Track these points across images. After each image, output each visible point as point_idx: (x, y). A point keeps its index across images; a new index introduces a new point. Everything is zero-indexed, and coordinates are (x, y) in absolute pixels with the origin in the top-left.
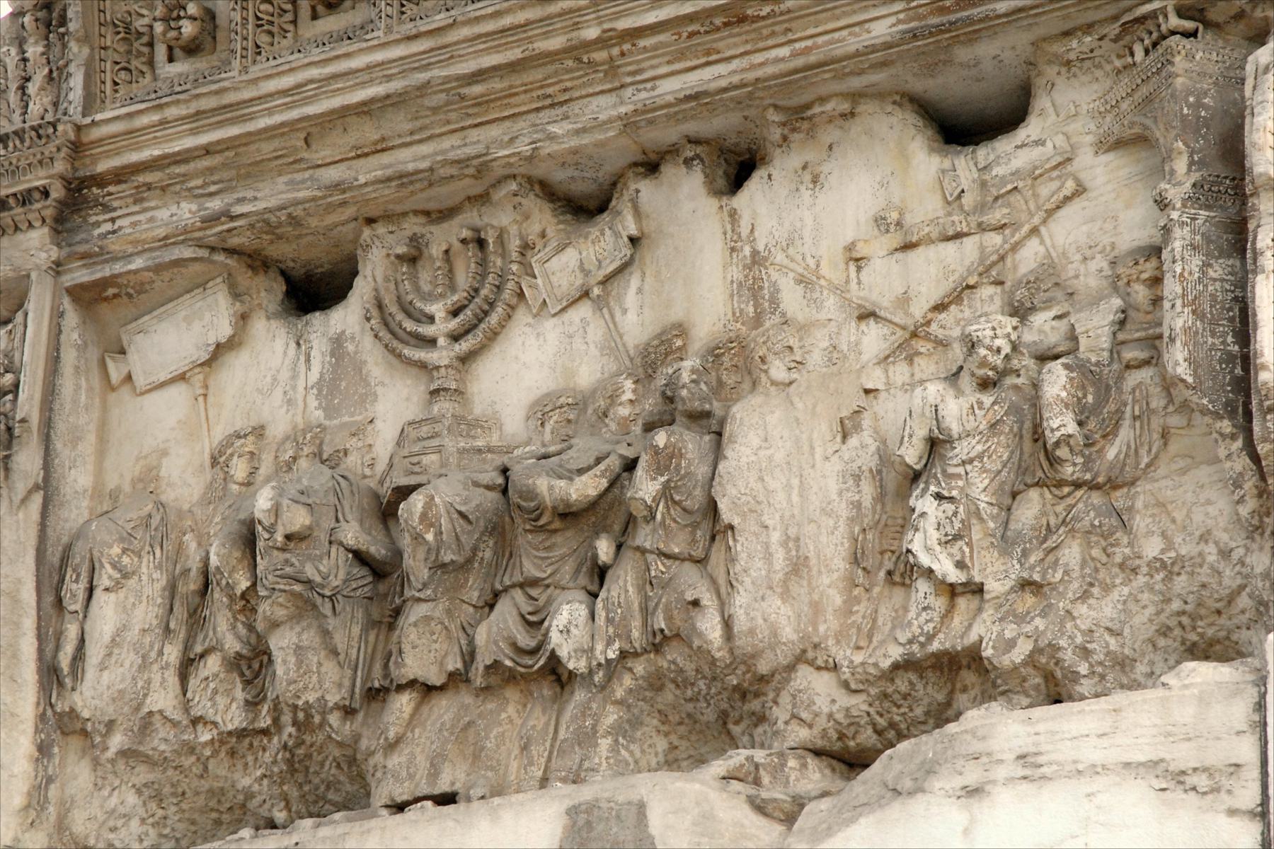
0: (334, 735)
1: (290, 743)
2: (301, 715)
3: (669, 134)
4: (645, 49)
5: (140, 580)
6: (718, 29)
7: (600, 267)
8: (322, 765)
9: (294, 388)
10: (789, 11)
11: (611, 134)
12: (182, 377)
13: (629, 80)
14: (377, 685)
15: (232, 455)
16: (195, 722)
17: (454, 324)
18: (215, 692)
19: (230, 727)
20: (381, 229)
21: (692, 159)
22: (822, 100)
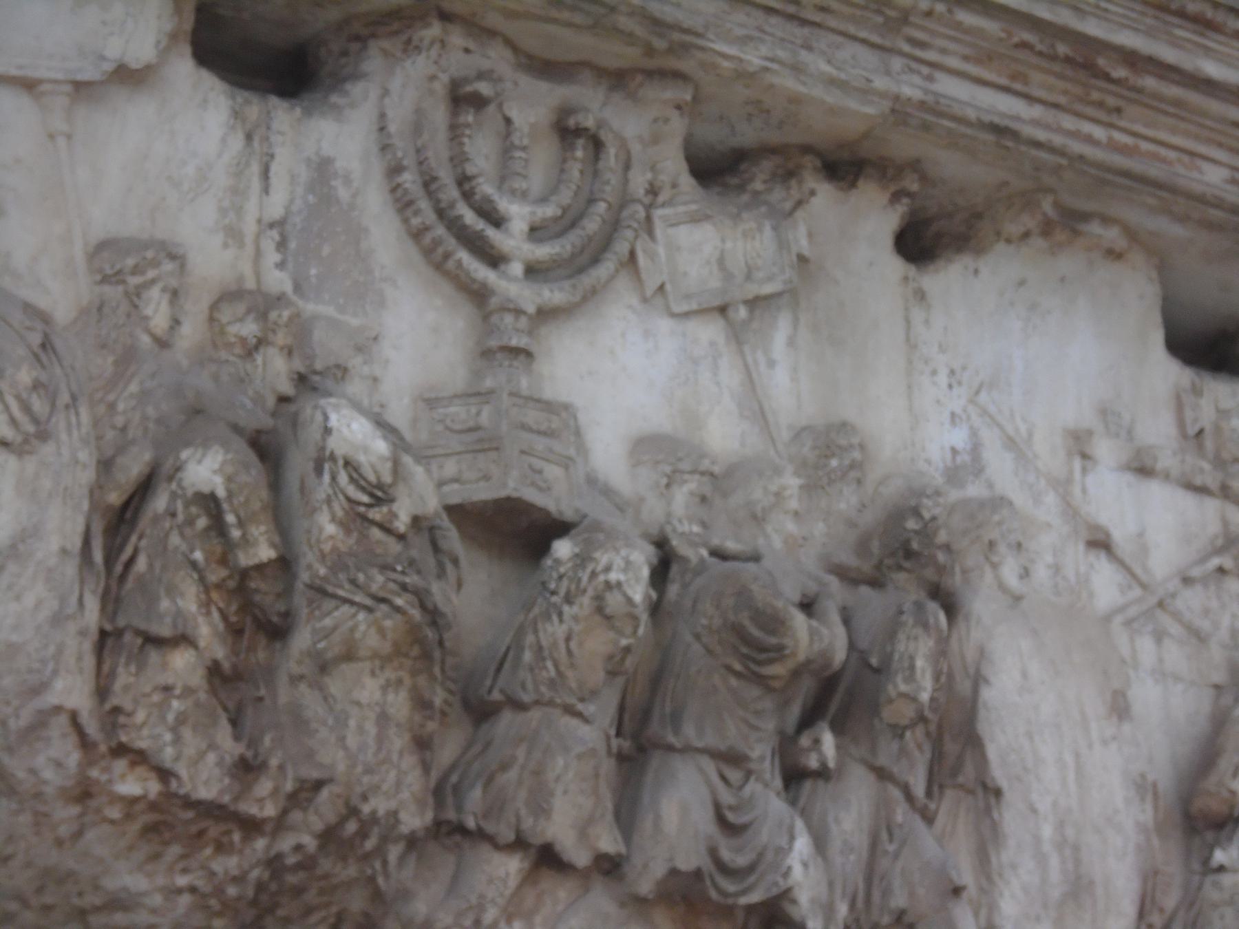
0: (380, 880)
1: (291, 860)
2: (351, 827)
3: (903, 145)
4: (958, 26)
5: (60, 454)
6: (1053, 58)
7: (749, 277)
8: (309, 911)
9: (239, 210)
10: (1140, 91)
11: (870, 110)
12: (29, 85)
13: (906, 48)
14: (471, 823)
15: (153, 282)
16: (120, 750)
17: (543, 252)
18: (181, 720)
19: (205, 793)
20: (457, 39)
21: (909, 194)
22: (1106, 220)
